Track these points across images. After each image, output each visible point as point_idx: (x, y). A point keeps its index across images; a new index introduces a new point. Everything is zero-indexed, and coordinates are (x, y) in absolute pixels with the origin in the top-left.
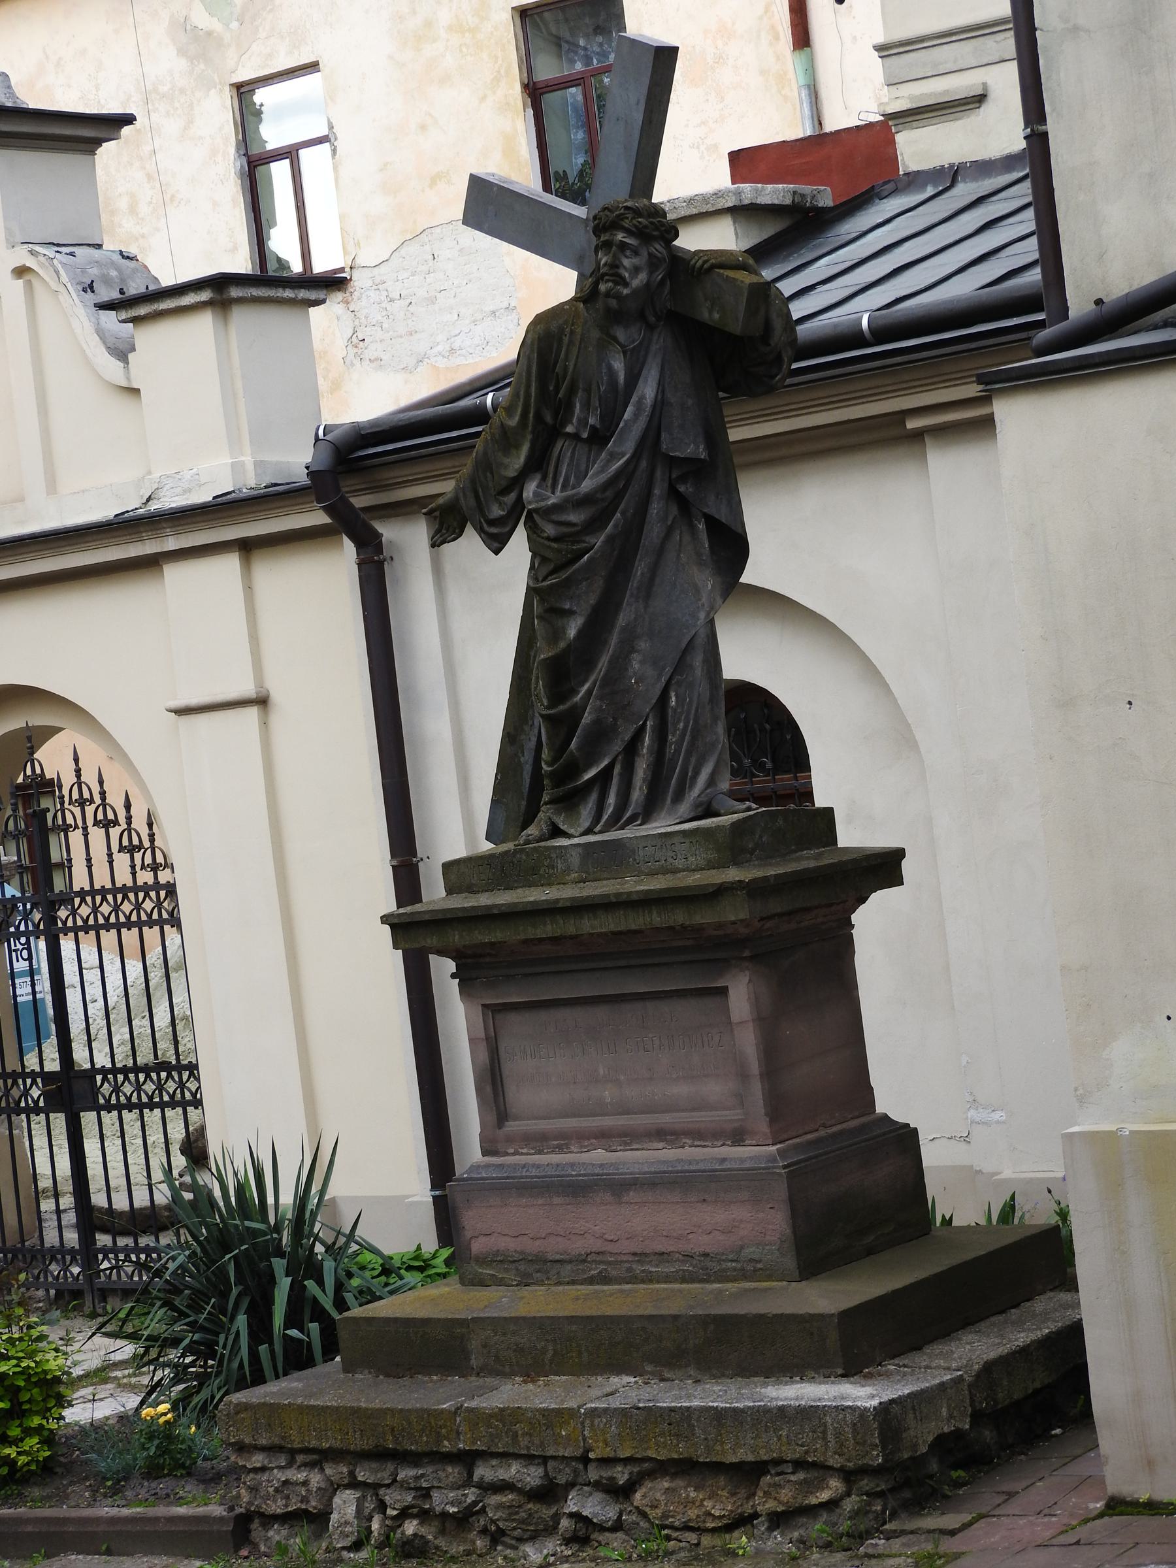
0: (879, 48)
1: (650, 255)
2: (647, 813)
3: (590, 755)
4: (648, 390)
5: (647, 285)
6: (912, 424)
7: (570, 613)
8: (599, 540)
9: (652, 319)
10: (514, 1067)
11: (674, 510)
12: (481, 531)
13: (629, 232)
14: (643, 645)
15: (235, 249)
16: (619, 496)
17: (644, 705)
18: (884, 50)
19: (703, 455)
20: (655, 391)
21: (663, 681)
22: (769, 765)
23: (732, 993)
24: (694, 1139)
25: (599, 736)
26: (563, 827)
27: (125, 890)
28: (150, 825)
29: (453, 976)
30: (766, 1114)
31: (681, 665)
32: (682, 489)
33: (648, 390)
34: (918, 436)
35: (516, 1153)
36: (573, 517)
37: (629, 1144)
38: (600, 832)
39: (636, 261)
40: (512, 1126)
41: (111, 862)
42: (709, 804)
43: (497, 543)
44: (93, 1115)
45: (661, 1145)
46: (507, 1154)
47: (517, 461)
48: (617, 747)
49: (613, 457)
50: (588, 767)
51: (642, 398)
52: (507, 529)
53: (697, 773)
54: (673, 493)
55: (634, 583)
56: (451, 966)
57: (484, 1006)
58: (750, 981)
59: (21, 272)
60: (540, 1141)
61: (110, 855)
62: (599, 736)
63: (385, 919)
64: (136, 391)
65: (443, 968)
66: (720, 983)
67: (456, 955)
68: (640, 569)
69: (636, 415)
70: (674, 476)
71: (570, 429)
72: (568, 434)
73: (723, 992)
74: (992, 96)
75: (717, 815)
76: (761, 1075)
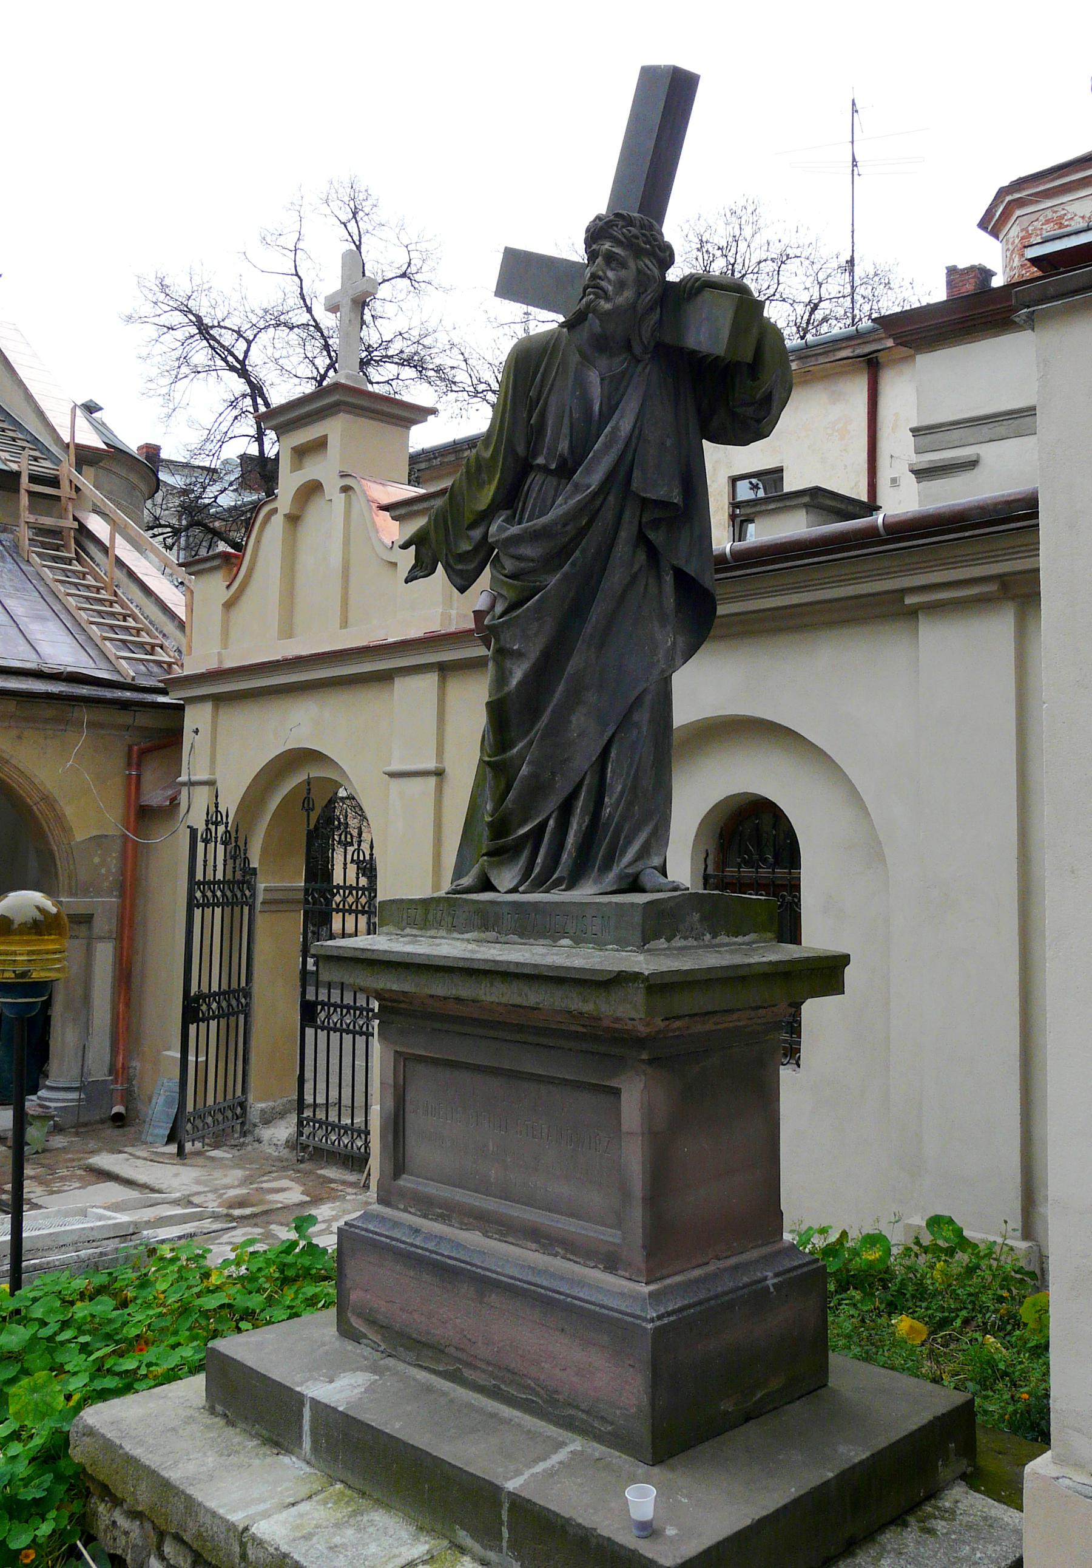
0: (912, 430)
1: (639, 271)
2: (573, 881)
4: (624, 423)
5: (633, 306)
6: (909, 600)
7: (519, 655)
8: (554, 580)
9: (637, 349)
10: (415, 1121)
11: (641, 557)
12: (448, 568)
13: (618, 242)
14: (591, 697)
16: (582, 532)
17: (582, 760)
18: (916, 431)
20: (632, 424)
21: (606, 738)
22: (771, 860)
23: (624, 1096)
24: (566, 1250)
25: (537, 789)
26: (495, 882)
27: (351, 887)
28: (372, 850)
30: (644, 1247)
31: (625, 722)
32: (652, 536)
33: (624, 423)
34: (913, 613)
35: (405, 1210)
36: (527, 551)
37: (505, 1235)
38: (523, 893)
39: (623, 273)
40: (406, 1182)
41: (345, 869)
42: (636, 877)
43: (463, 582)
44: (312, 1030)
45: (534, 1246)
46: (398, 1209)
47: (486, 496)
48: (553, 803)
49: (577, 488)
50: (521, 824)
51: (616, 428)
52: (471, 566)
53: (629, 842)
54: (642, 539)
55: (588, 629)
57: (396, 1052)
58: (645, 1087)
59: (346, 489)
60: (426, 1206)
61: (345, 864)
62: (537, 789)
64: (395, 564)
66: (614, 1083)
68: (597, 613)
69: (607, 446)
71: (540, 460)
73: (616, 1092)
74: (982, 462)
75: (643, 890)
76: (643, 1198)
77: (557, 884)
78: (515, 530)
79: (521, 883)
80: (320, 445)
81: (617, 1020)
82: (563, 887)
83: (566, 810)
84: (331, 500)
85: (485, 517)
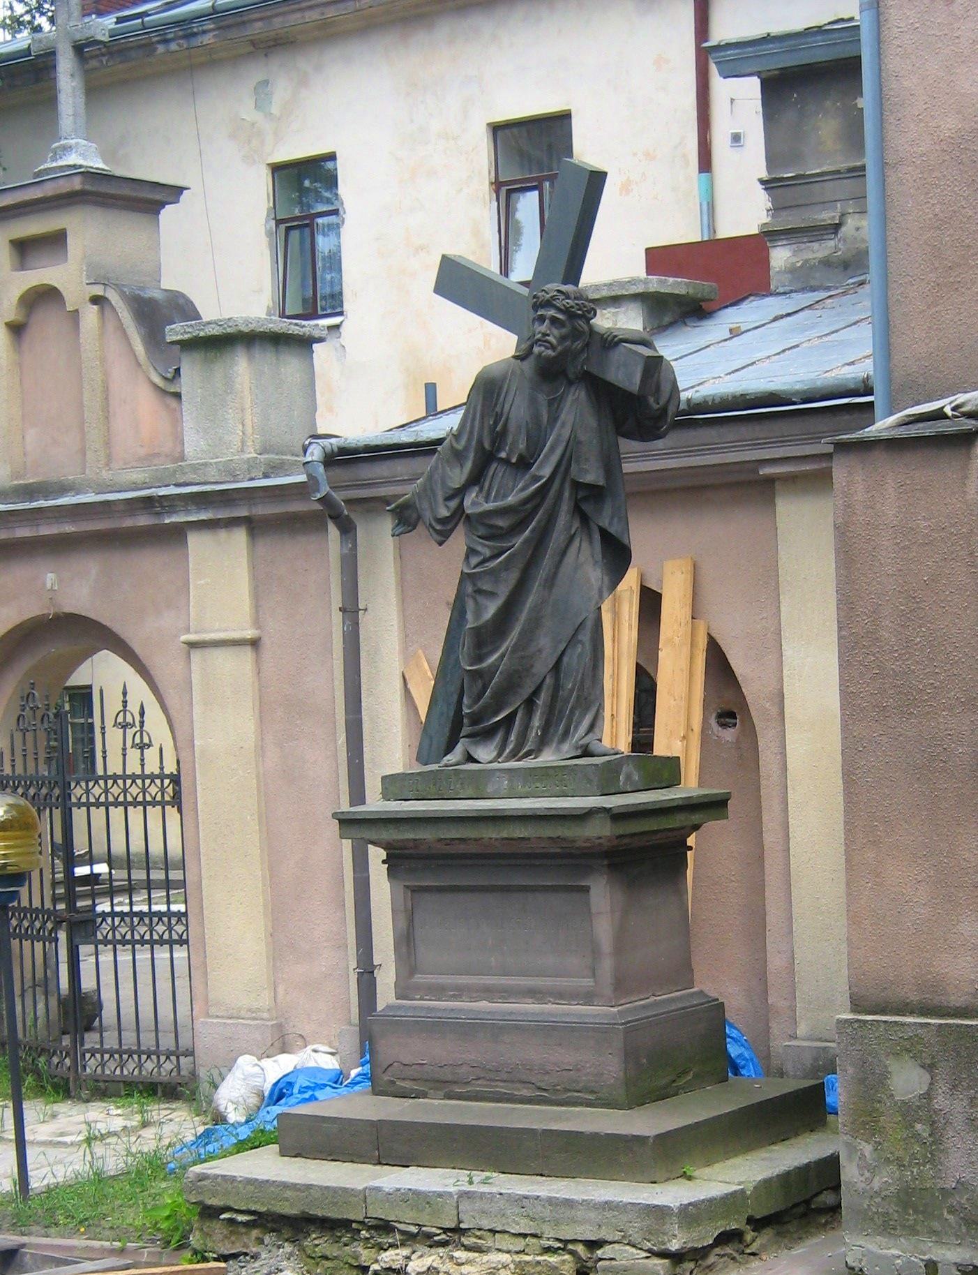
3: (499, 701)
7: (492, 595)
8: (519, 541)
11: (576, 524)
13: (559, 310)
15: (261, 290)
17: (542, 667)
19: (601, 482)
24: (556, 998)
29: (384, 862)
31: (573, 640)
32: (584, 507)
35: (421, 999)
40: (419, 978)
52: (449, 527)
56: (382, 854)
59: (96, 300)
63: (335, 815)
65: (377, 855)
67: (387, 846)
70: (579, 497)
71: (503, 455)
72: (501, 459)
73: (586, 890)
75: (592, 756)
77: (527, 755)
78: (490, 506)
79: (499, 755)
80: (57, 240)
81: (588, 840)
82: (532, 757)
83: (530, 703)
84: (77, 311)
85: (461, 492)
